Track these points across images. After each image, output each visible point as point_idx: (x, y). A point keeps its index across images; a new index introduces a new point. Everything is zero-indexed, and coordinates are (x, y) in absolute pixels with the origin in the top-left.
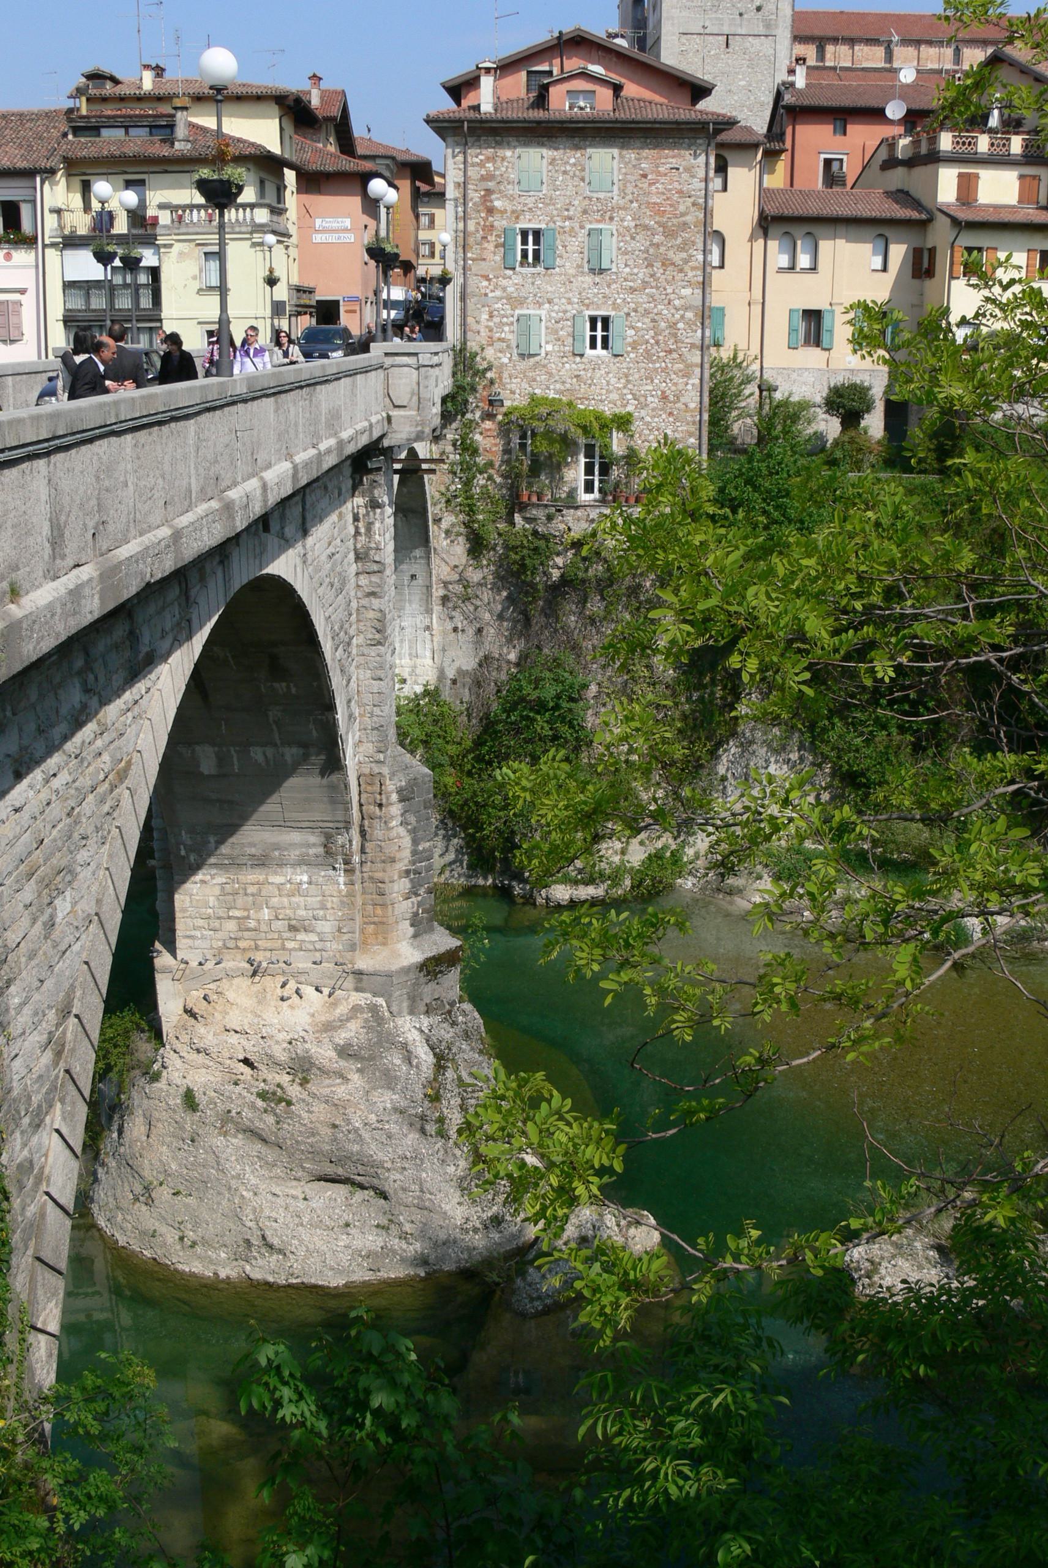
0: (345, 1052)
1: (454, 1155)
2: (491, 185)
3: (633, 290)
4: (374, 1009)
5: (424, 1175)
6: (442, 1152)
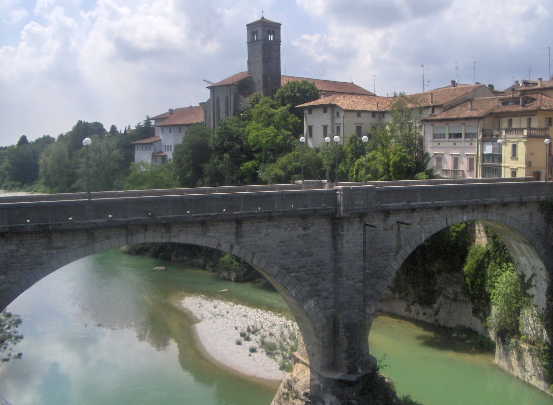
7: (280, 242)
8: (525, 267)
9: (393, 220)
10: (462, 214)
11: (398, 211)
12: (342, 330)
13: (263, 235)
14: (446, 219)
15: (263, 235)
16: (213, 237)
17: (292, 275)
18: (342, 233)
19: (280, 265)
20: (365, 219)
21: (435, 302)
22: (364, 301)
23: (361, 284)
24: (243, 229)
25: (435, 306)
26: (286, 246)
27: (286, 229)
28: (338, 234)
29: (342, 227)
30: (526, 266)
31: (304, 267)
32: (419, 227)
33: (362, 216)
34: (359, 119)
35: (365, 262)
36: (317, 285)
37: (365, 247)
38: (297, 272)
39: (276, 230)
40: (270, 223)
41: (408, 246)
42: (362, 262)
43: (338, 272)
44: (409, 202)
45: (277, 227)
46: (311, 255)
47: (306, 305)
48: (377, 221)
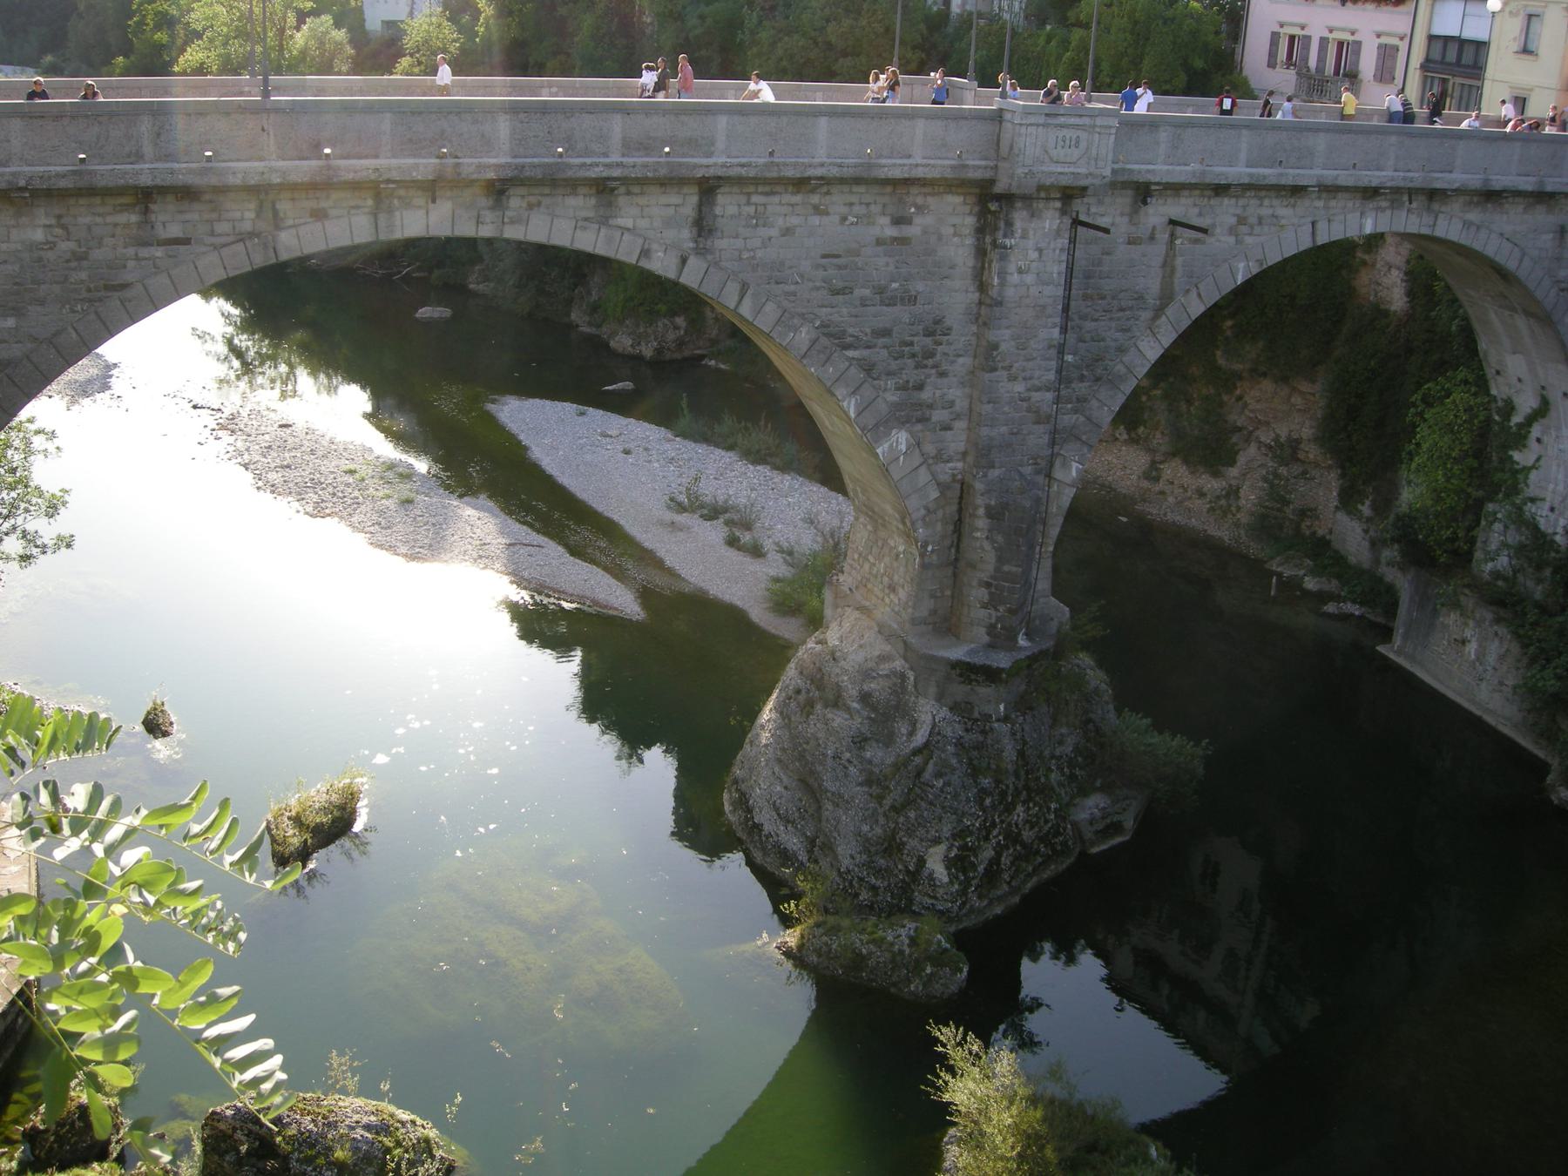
0: (865, 698)
1: (877, 821)
4: (903, 677)
5: (844, 818)
6: (870, 812)
7: (824, 256)
8: (1519, 385)
9: (1158, 213)
10: (1362, 214)
12: (981, 524)
13: (774, 232)
14: (1313, 224)
15: (774, 232)
16: (628, 230)
17: (851, 353)
18: (1008, 242)
19: (818, 323)
20: (1079, 206)
21: (1232, 462)
22: (1053, 443)
23: (1049, 396)
24: (718, 210)
25: (1233, 472)
26: (839, 267)
27: (844, 219)
28: (994, 244)
29: (1009, 224)
30: (1520, 380)
31: (886, 333)
32: (1232, 240)
35: (1064, 330)
36: (920, 387)
37: (1068, 286)
38: (868, 347)
39: (816, 220)
40: (798, 198)
41: (1193, 294)
42: (1056, 332)
43: (988, 357)
45: (817, 210)
46: (913, 300)
47: (886, 445)
48: (1111, 213)
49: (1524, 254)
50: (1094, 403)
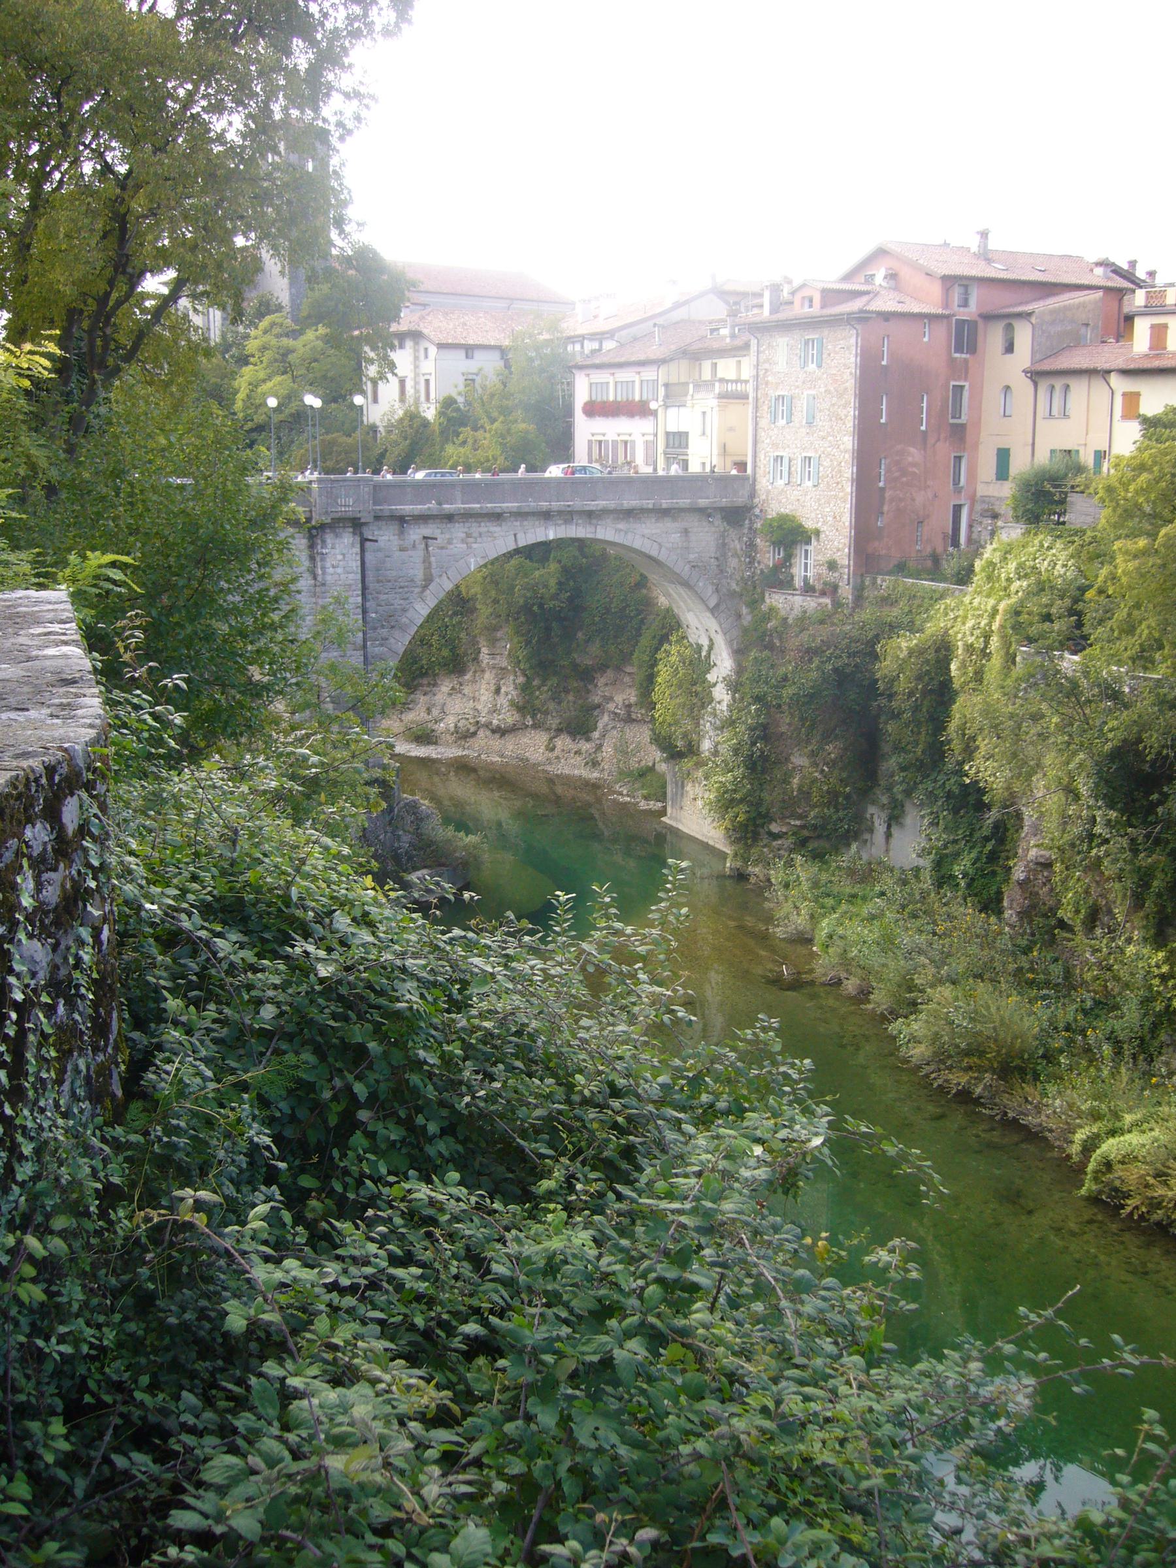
2: (767, 366)
3: (823, 438)
11: (424, 518)
25: (596, 735)
29: (324, 542)
33: (356, 524)
34: (469, 362)
44: (440, 504)
49: (660, 546)
50: (392, 640)
